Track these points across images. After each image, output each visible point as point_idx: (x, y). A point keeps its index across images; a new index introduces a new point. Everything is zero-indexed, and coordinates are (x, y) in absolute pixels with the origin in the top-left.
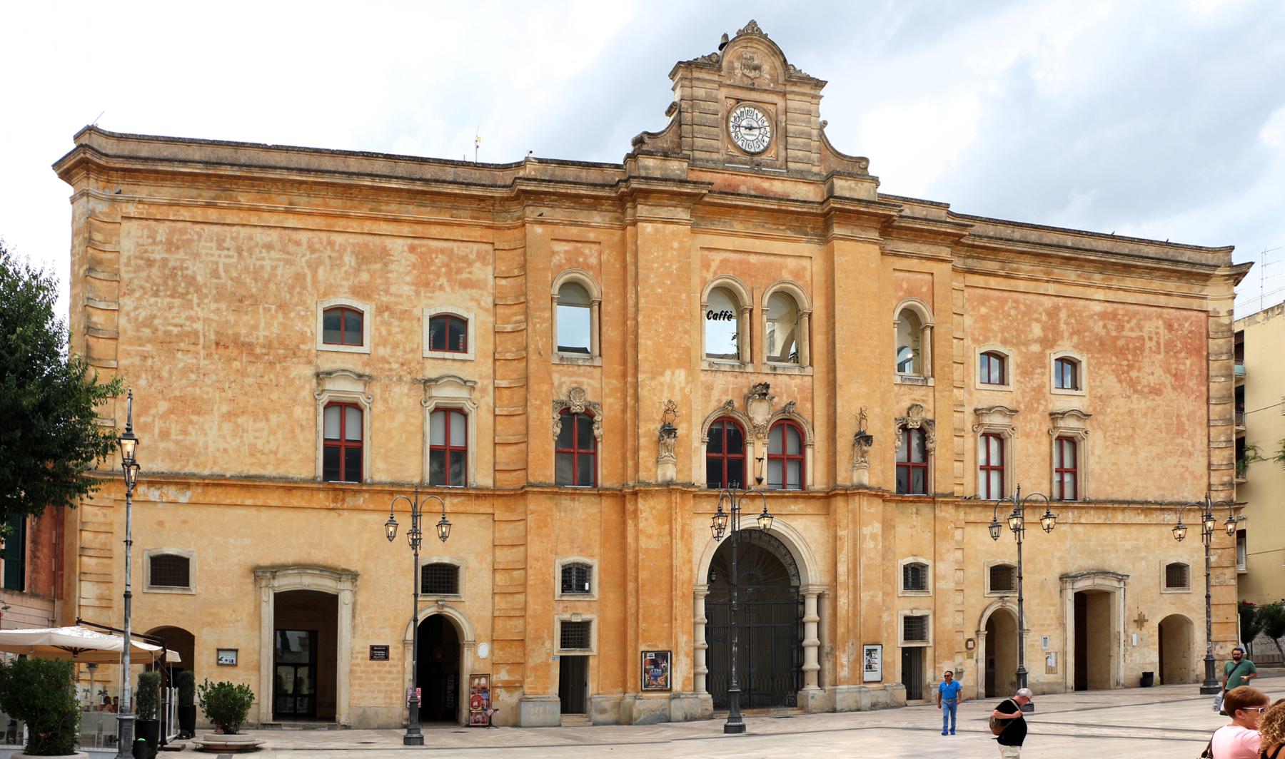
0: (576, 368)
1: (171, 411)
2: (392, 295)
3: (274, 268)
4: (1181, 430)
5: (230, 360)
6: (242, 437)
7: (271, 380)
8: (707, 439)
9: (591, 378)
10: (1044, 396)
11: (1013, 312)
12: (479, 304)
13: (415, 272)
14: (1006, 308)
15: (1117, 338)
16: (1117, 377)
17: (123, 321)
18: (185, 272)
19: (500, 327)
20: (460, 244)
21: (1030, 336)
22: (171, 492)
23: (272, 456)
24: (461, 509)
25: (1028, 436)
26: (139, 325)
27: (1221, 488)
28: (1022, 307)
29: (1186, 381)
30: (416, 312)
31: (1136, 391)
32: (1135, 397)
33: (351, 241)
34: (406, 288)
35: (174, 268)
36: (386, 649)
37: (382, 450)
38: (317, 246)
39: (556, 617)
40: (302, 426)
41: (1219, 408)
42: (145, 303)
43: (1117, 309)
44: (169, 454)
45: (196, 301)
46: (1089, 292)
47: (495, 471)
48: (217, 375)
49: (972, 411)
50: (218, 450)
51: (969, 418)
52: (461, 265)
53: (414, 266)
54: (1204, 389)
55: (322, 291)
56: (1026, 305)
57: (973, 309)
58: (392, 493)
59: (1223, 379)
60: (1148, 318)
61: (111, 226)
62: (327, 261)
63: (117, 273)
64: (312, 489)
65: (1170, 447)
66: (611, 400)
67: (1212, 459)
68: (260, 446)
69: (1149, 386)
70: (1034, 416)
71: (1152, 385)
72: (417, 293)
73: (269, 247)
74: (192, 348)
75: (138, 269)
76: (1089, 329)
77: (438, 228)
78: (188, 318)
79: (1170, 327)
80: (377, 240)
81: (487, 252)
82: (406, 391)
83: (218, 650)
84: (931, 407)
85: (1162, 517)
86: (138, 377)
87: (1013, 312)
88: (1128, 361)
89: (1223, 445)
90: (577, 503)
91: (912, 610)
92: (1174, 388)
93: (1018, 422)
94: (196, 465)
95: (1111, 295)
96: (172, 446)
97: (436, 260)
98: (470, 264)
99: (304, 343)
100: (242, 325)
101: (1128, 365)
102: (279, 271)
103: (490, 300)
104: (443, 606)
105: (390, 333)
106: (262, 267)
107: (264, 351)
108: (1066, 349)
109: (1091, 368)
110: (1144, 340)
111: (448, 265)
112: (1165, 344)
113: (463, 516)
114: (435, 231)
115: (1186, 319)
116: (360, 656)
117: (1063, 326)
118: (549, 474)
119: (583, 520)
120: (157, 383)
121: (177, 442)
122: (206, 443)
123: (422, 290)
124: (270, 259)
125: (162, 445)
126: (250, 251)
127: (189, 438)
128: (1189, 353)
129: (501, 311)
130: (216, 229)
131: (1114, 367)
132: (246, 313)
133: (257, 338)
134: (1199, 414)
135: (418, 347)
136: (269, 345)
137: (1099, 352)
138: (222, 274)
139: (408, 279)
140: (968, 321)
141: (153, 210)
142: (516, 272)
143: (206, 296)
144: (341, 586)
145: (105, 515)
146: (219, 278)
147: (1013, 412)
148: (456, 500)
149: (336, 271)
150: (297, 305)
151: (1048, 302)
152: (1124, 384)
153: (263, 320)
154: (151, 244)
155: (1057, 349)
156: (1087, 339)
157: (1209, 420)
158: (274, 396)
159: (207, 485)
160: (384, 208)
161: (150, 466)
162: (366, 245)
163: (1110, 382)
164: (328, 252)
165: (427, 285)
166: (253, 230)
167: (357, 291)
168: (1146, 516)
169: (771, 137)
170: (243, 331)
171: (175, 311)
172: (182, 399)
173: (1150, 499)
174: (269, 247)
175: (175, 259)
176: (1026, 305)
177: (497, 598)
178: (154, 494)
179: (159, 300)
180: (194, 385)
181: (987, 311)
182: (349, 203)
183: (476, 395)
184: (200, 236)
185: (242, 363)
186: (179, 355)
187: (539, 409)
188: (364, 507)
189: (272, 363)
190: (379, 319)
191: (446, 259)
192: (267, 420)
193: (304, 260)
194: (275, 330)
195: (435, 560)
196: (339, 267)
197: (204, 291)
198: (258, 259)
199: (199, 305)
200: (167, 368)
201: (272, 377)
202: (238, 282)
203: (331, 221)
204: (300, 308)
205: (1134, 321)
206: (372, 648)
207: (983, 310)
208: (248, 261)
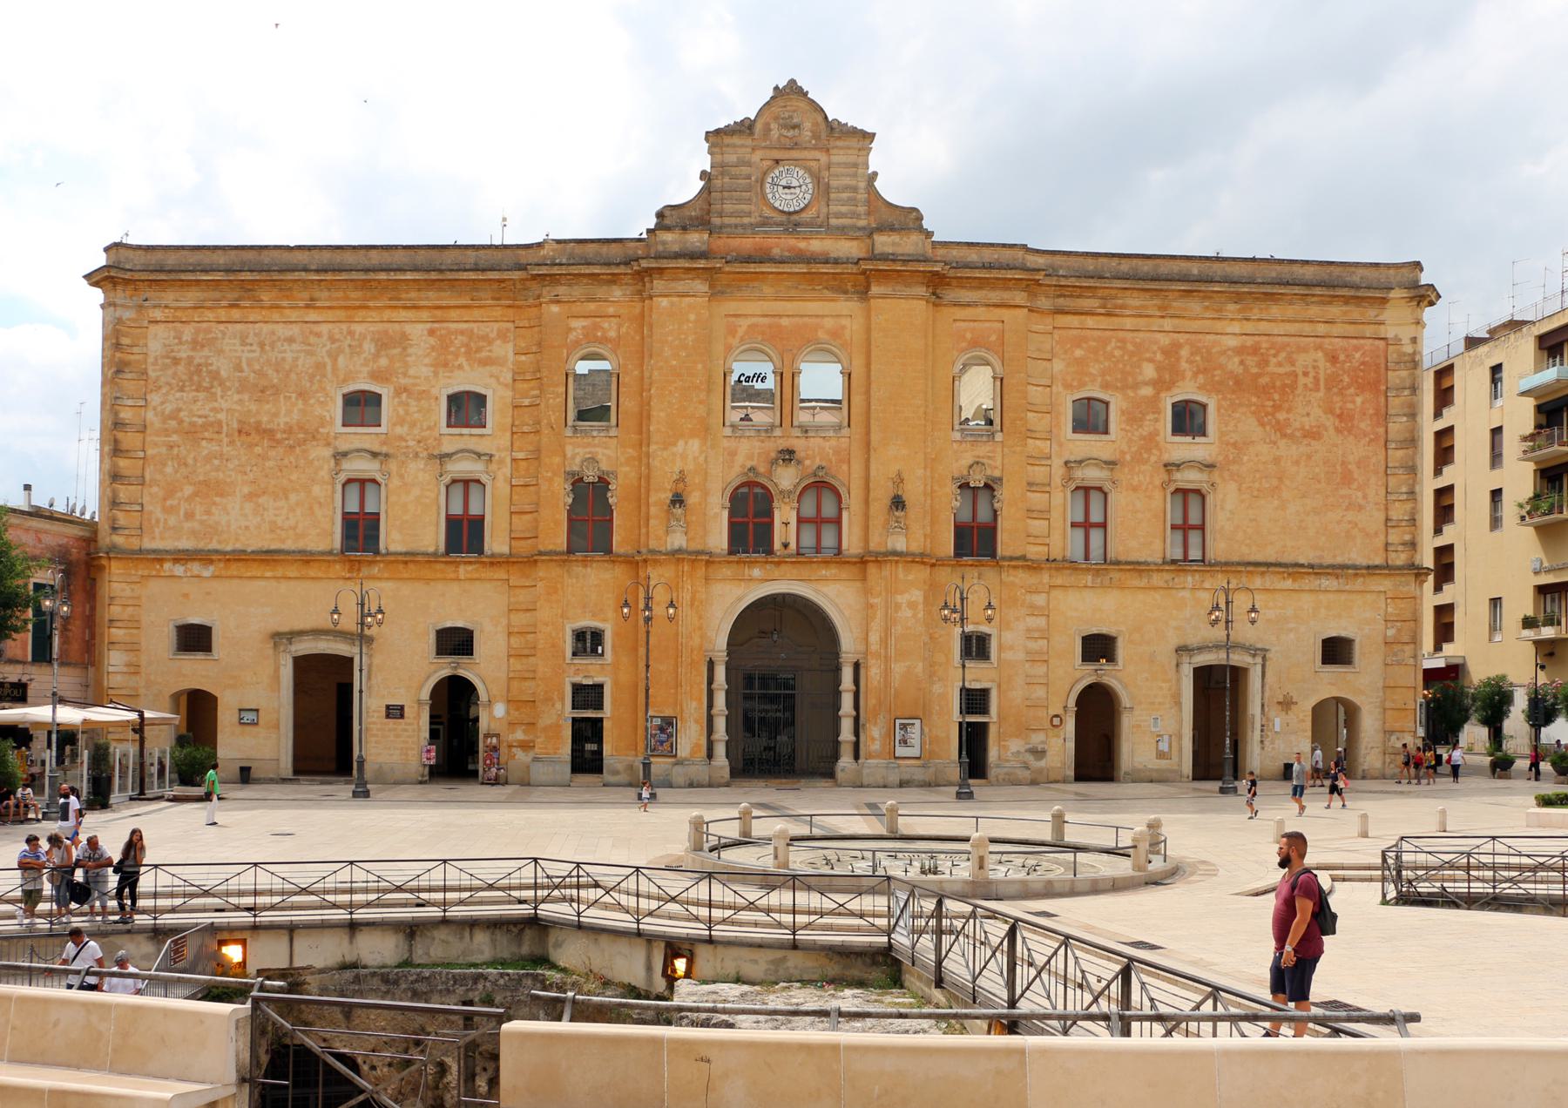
0: (590, 440)
1: (196, 494)
2: (409, 377)
3: (296, 359)
5: (251, 446)
6: (262, 515)
7: (291, 462)
8: (728, 505)
9: (606, 448)
10: (1157, 446)
11: (1117, 353)
12: (498, 379)
13: (434, 354)
14: (1109, 348)
15: (1259, 375)
16: (1259, 421)
17: (150, 415)
18: (210, 368)
19: (518, 402)
20: (480, 324)
21: (1140, 378)
22: (195, 568)
23: (291, 532)
24: (476, 575)
25: (1135, 489)
26: (166, 418)
28: (1130, 347)
29: (1356, 422)
30: (434, 391)
31: (1284, 435)
32: (1282, 443)
33: (371, 329)
34: (424, 369)
35: (200, 365)
37: (398, 523)
38: (337, 337)
40: (320, 503)
41: (1400, 453)
42: (171, 397)
44: (193, 533)
45: (219, 393)
47: (511, 538)
48: (239, 460)
49: (1061, 462)
50: (240, 528)
51: (1058, 472)
52: (481, 344)
53: (433, 348)
54: (1381, 430)
55: (342, 377)
58: (406, 563)
59: (1405, 419)
61: (139, 330)
62: (347, 350)
63: (145, 372)
64: (329, 561)
68: (279, 523)
69: (1302, 428)
70: (1143, 468)
71: (1307, 427)
72: (436, 374)
73: (291, 340)
74: (216, 436)
75: (165, 368)
76: (1221, 367)
77: (458, 312)
80: (397, 326)
81: (508, 330)
82: (422, 466)
84: (999, 463)
86: (165, 465)
87: (1117, 353)
88: (1274, 401)
89: (1405, 497)
90: (589, 569)
92: (1338, 431)
93: (1123, 475)
94: (219, 542)
96: (196, 525)
97: (456, 342)
98: (490, 343)
99: (323, 427)
101: (1273, 406)
102: (300, 362)
103: (507, 377)
105: (407, 413)
106: (283, 359)
107: (284, 436)
108: (1187, 391)
109: (1222, 411)
110: (1296, 376)
111: (467, 345)
112: (1326, 380)
113: (478, 582)
114: (454, 314)
117: (1184, 365)
118: (559, 541)
119: (596, 586)
120: (183, 470)
121: (202, 522)
123: (441, 370)
124: (291, 351)
125: (187, 525)
126: (272, 345)
128: (1361, 388)
129: (519, 385)
130: (239, 326)
131: (1253, 408)
132: (268, 402)
133: (278, 425)
134: (1374, 460)
135: (435, 424)
136: (289, 430)
137: (1234, 392)
138: (244, 365)
139: (427, 361)
140: (1058, 366)
141: (178, 314)
142: (534, 349)
143: (230, 389)
145: (133, 590)
146: (242, 371)
147: (1111, 464)
148: (470, 568)
149: (355, 359)
150: (317, 392)
152: (1268, 428)
153: (284, 408)
154: (177, 344)
155: (1175, 391)
156: (1217, 378)
157: (1387, 467)
158: (294, 477)
159: (229, 560)
160: (404, 296)
161: (176, 544)
162: (386, 332)
163: (1248, 426)
164: (349, 341)
165: (446, 365)
166: (275, 327)
167: (376, 376)
169: (812, 194)
171: (199, 404)
172: (206, 483)
174: (291, 340)
178: (179, 570)
179: (185, 394)
180: (217, 469)
181: (1083, 353)
182: (369, 294)
183: (494, 467)
184: (224, 334)
185: (263, 449)
186: (204, 443)
187: (550, 480)
188: (379, 575)
189: (292, 447)
190: (396, 400)
192: (287, 498)
193: (324, 349)
194: (295, 416)
196: (359, 354)
197: (228, 384)
198: (281, 352)
200: (192, 456)
201: (292, 459)
202: (260, 374)
203: (350, 312)
204: (320, 395)
207: (1079, 353)
208: (270, 354)
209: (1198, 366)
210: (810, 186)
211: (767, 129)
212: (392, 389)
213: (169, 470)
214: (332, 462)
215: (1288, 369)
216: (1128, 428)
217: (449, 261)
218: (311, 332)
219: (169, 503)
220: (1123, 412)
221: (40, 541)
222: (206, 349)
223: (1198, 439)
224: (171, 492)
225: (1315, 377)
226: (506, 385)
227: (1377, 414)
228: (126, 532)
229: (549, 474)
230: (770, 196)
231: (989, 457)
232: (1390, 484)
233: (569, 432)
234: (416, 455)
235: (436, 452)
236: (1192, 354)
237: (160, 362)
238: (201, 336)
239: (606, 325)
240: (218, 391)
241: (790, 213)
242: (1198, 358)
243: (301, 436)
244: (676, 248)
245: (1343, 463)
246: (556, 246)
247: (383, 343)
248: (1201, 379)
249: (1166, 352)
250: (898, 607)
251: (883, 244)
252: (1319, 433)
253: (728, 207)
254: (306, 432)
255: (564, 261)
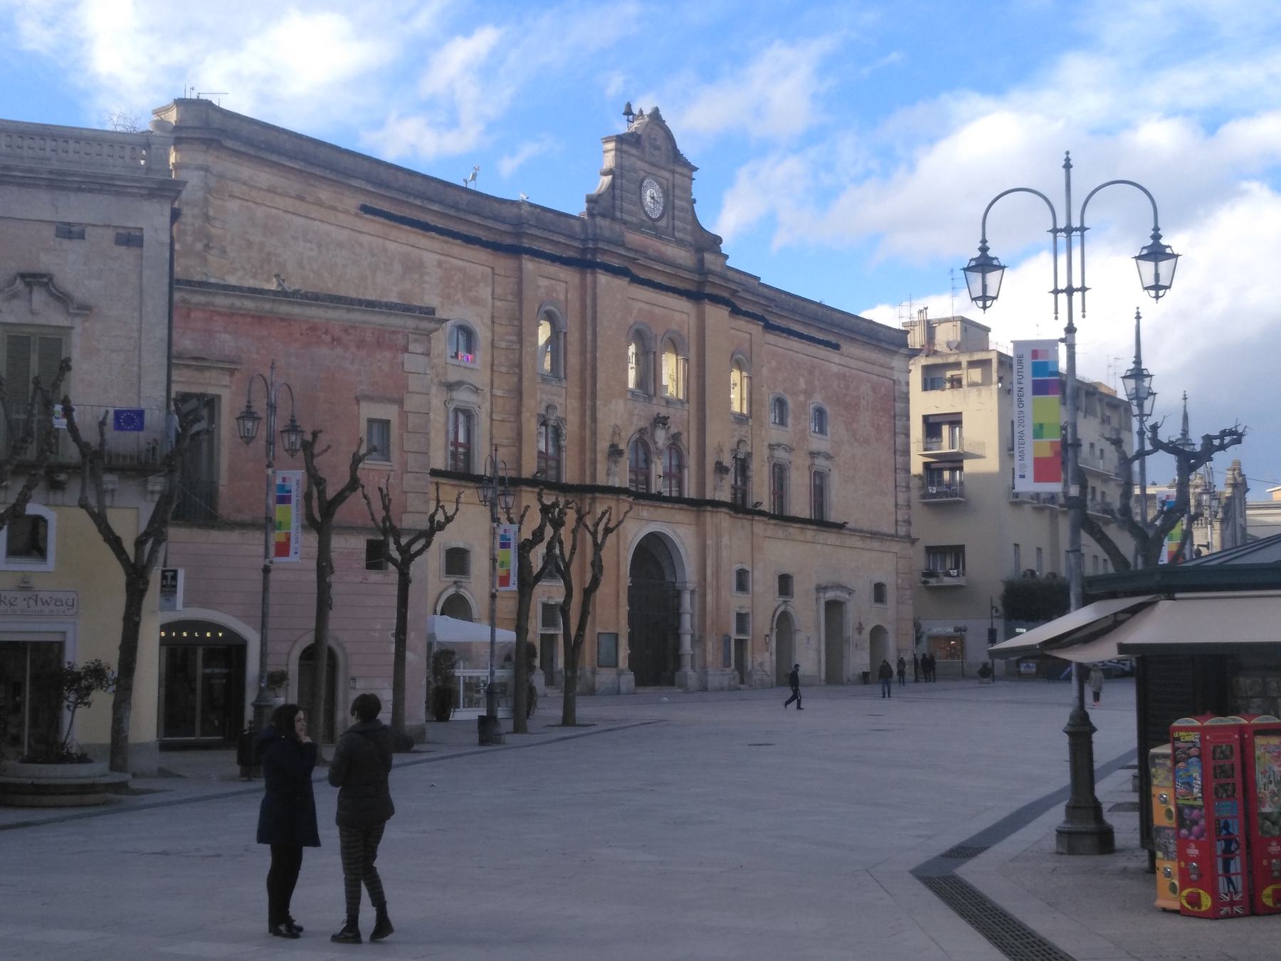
27: (903, 524)
39: (538, 599)
54: (892, 442)
67: (898, 500)
91: (740, 608)
104: (460, 587)
246: (528, 208)
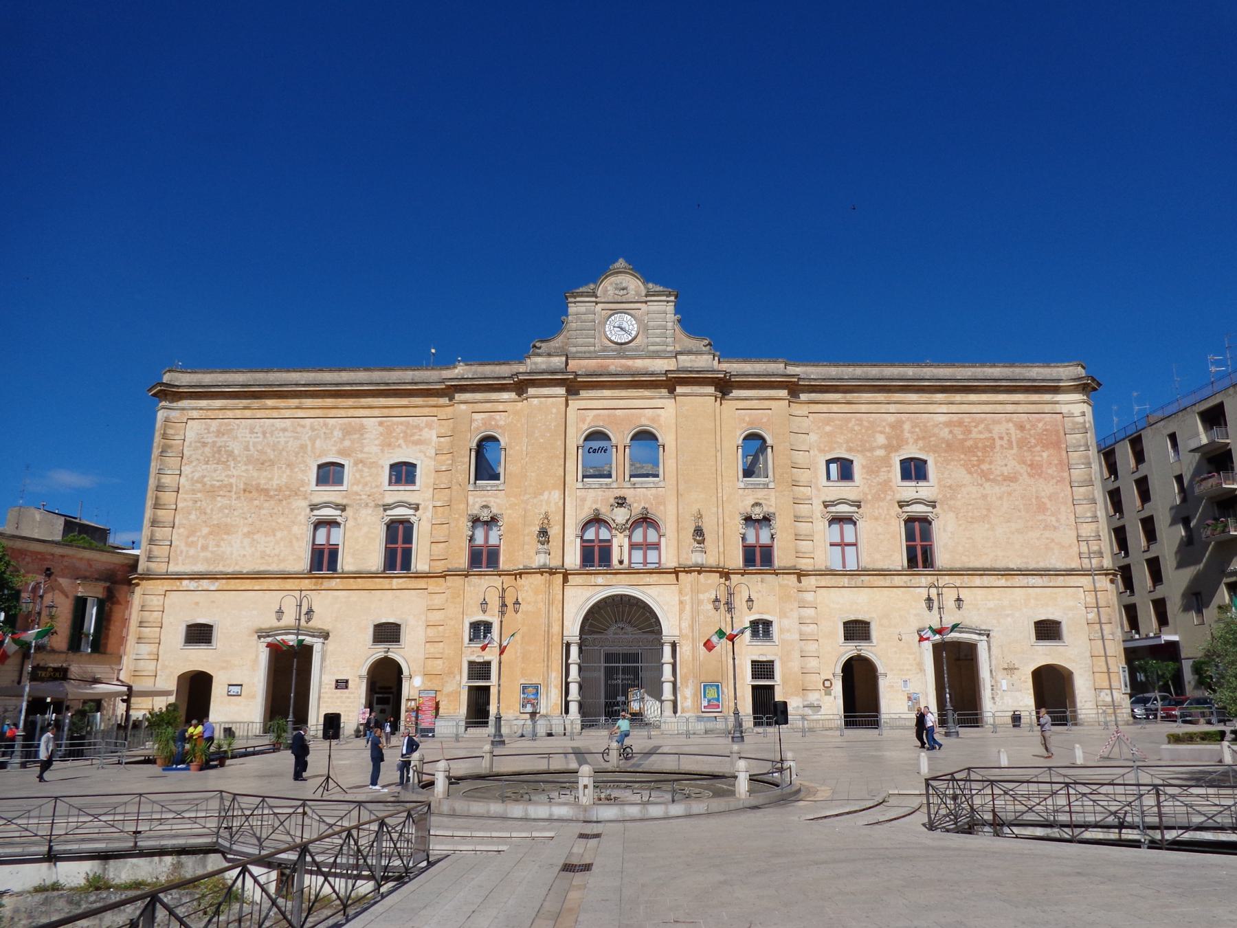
1: (211, 533)
3: (287, 442)
4: (1042, 508)
5: (252, 500)
9: (496, 498)
10: (891, 488)
11: (856, 428)
14: (850, 425)
16: (967, 470)
21: (875, 444)
23: (276, 558)
25: (876, 519)
26: (194, 482)
28: (866, 424)
30: (381, 462)
31: (988, 480)
32: (987, 485)
35: (220, 447)
36: (347, 681)
38: (316, 427)
42: (199, 469)
43: (962, 418)
44: (207, 560)
45: (232, 465)
46: (931, 408)
50: (240, 555)
51: (818, 508)
53: (381, 434)
54: (1066, 474)
56: (869, 422)
57: (819, 428)
59: (1083, 466)
60: (999, 422)
62: (322, 435)
65: (1030, 523)
66: (509, 511)
70: (881, 504)
71: (1006, 474)
72: (382, 451)
74: (227, 494)
75: (196, 449)
76: (934, 435)
78: (226, 476)
79: (1021, 428)
81: (433, 421)
83: (229, 685)
85: (1026, 581)
86: (190, 514)
87: (856, 428)
89: (1090, 520)
92: (1029, 475)
95: (954, 408)
96: (208, 554)
98: (421, 430)
99: (303, 486)
100: (263, 478)
102: (290, 444)
103: (433, 452)
104: (387, 652)
105: (362, 477)
107: (276, 493)
108: (911, 451)
109: (939, 464)
110: (994, 439)
111: (405, 432)
115: (1039, 421)
116: (328, 686)
117: (907, 435)
121: (212, 552)
122: (232, 554)
123: (386, 449)
124: (285, 437)
125: (202, 554)
126: (272, 434)
127: (221, 549)
128: (1046, 447)
129: (439, 457)
132: (266, 471)
136: (279, 489)
137: (946, 451)
138: (251, 448)
139: (377, 442)
140: (813, 437)
143: (240, 462)
144: (315, 640)
145: (158, 600)
147: (858, 504)
150: (300, 463)
151: (891, 418)
152: (975, 475)
155: (901, 452)
156: (933, 443)
158: (280, 520)
163: (960, 474)
164: (324, 430)
165: (389, 445)
167: (341, 453)
168: (1006, 580)
170: (263, 482)
172: (218, 526)
173: (1011, 566)
174: (284, 430)
175: (220, 441)
176: (869, 422)
177: (428, 645)
180: (227, 517)
184: (238, 425)
186: (219, 498)
189: (280, 501)
191: (403, 428)
192: (274, 535)
193: (307, 436)
195: (384, 620)
197: (239, 459)
199: (234, 468)
201: (280, 509)
202: (261, 452)
205: (981, 427)
206: (337, 681)
207: (828, 429)
208: (270, 439)
209: (918, 435)
210: (635, 326)
211: (606, 291)
212: (352, 461)
213: (193, 517)
214: (308, 510)
215: (987, 435)
216: (868, 477)
217: (395, 378)
218: (298, 425)
219: (190, 539)
220: (863, 467)
221: (91, 566)
222: (226, 436)
223: (921, 484)
224: (192, 532)
225: (1008, 440)
226: (431, 458)
227: (1061, 463)
228: (158, 560)
229: (457, 516)
230: (608, 333)
231: (765, 499)
232: (1077, 511)
233: (471, 487)
234: (367, 505)
235: (380, 503)
236: (912, 427)
237: (193, 445)
238: (223, 428)
239: (498, 417)
240: (232, 464)
241: (622, 344)
242: (917, 430)
243: (287, 493)
244: (544, 367)
245: (1037, 497)
247: (347, 432)
248: (921, 443)
249: (892, 426)
250: (699, 602)
251: (685, 360)
252: (1015, 477)
253: (580, 341)
254: (291, 490)
255: (470, 376)
